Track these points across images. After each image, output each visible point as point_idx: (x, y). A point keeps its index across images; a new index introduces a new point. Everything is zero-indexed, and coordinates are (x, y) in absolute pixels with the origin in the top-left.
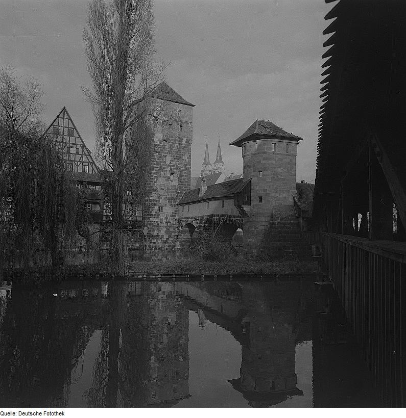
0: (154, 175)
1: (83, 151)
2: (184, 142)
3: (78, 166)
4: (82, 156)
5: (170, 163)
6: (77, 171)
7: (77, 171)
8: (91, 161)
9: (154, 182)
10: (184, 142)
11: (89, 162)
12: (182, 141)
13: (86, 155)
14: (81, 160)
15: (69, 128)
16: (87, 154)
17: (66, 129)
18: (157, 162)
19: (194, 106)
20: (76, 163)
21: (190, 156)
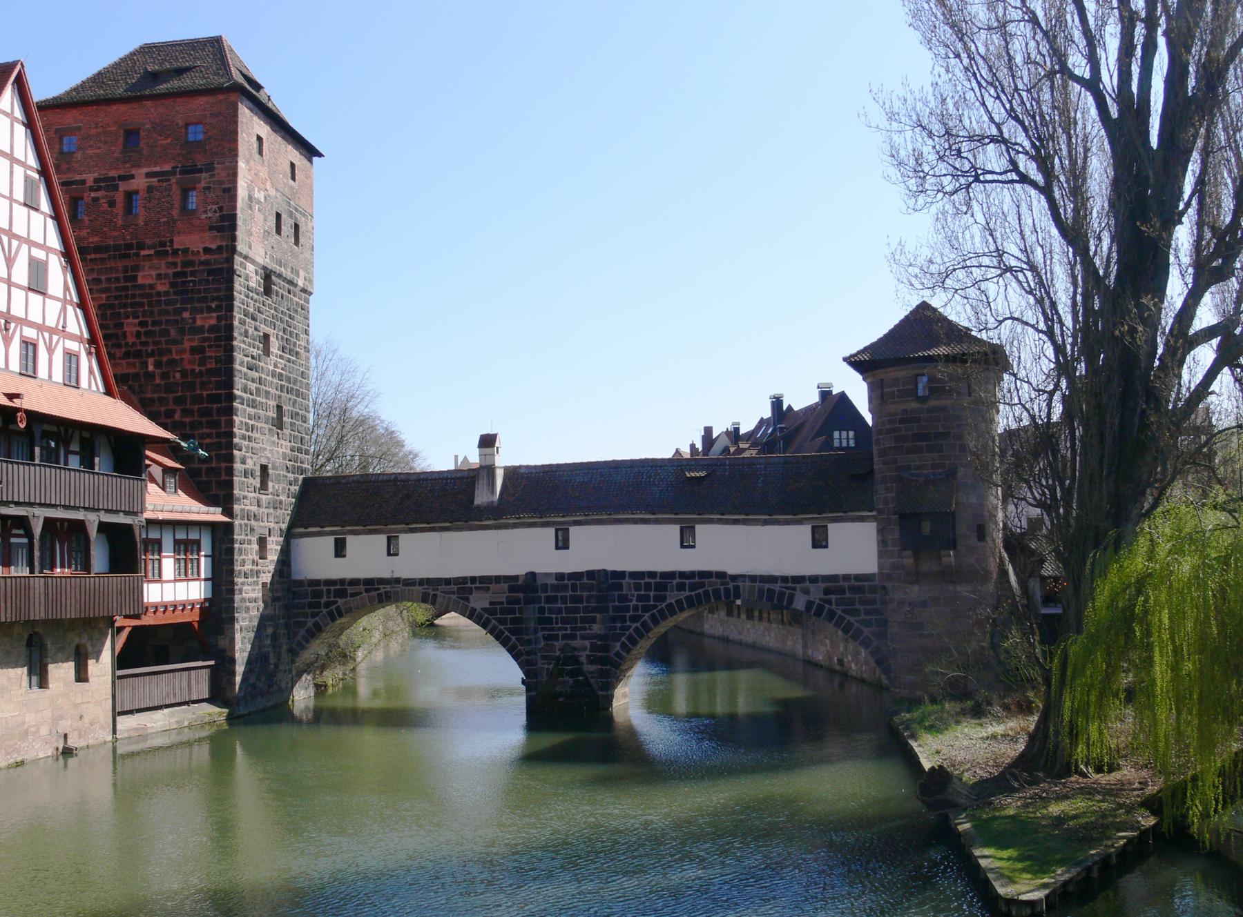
0: (248, 409)
1: (66, 288)
3: (50, 351)
4: (65, 302)
5: (276, 366)
6: (50, 377)
7: (50, 377)
8: (86, 335)
11: (79, 339)
12: (296, 285)
14: (60, 328)
15: (23, 164)
16: (75, 299)
17: (19, 172)
18: (253, 357)
20: (47, 335)
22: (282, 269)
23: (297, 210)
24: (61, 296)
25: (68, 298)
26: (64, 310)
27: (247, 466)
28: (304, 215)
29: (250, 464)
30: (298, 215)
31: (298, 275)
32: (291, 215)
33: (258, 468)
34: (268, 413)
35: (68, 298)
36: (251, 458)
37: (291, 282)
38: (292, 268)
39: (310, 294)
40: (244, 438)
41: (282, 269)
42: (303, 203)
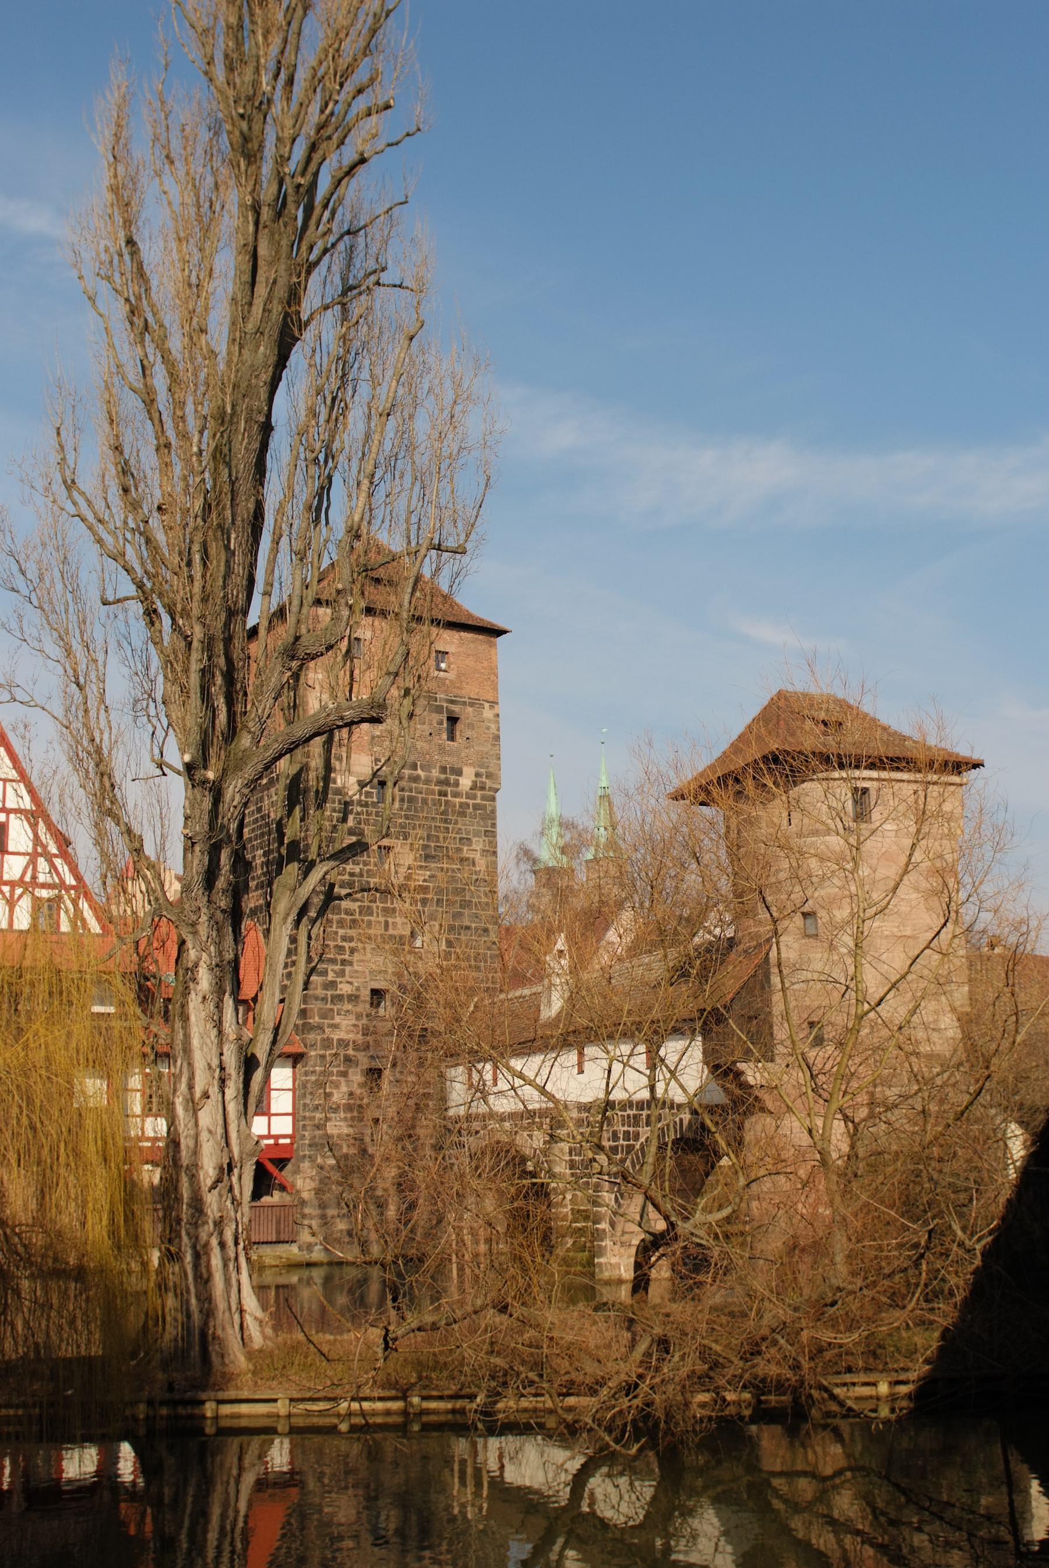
0: (341, 932)
2: (466, 782)
4: (33, 858)
5: (408, 878)
8: (70, 880)
9: (344, 962)
10: (466, 782)
12: (457, 784)
13: (49, 858)
14: (27, 878)
16: (53, 849)
18: (352, 874)
19: (499, 632)
21: (493, 844)
22: (420, 772)
23: (452, 702)
24: (30, 850)
25: (39, 850)
26: (33, 863)
27: (338, 992)
28: (472, 705)
29: (345, 989)
30: (456, 708)
31: (459, 772)
32: (439, 710)
33: (366, 994)
34: (391, 932)
35: (39, 850)
36: (351, 983)
37: (446, 782)
38: (443, 770)
39: (497, 790)
40: (333, 961)
41: (420, 772)
42: (470, 690)
